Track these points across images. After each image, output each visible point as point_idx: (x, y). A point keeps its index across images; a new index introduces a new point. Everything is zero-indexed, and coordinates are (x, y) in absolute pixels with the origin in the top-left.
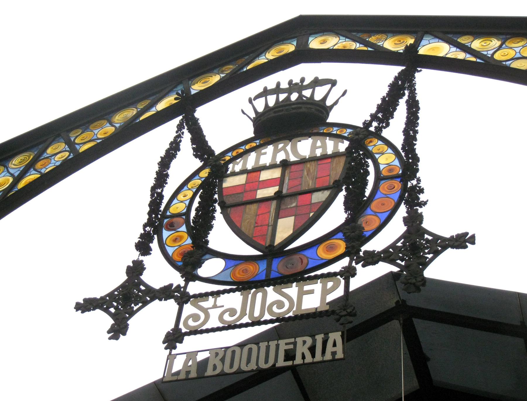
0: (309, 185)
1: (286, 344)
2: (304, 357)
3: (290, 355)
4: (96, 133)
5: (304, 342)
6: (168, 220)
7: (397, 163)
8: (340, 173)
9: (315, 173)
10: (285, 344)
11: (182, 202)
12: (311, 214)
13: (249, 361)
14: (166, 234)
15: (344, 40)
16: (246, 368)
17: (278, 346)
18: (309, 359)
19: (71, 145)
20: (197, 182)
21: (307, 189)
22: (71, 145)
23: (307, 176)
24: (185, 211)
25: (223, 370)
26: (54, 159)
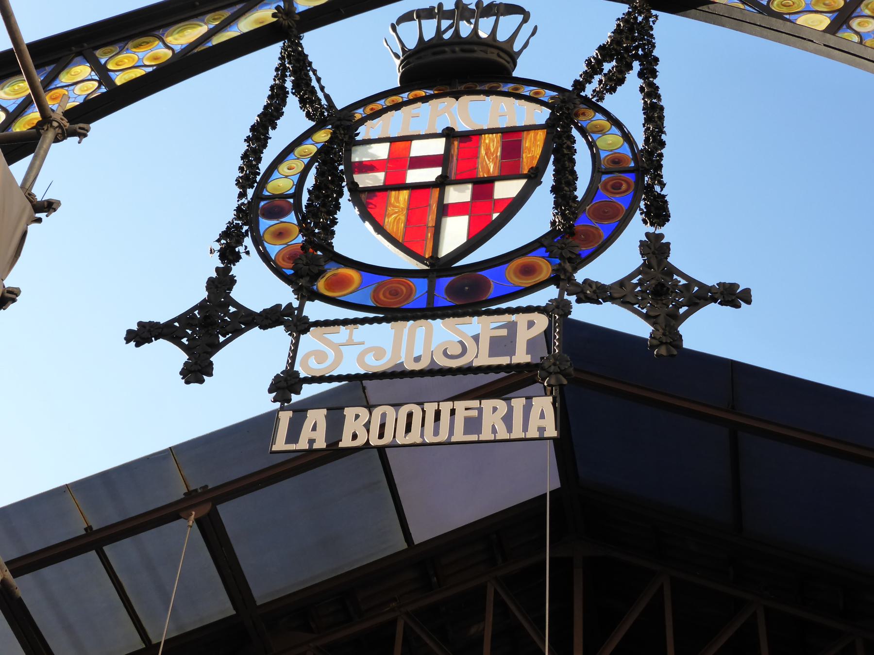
0: (489, 170)
2: (494, 431)
3: (473, 424)
6: (265, 202)
7: (627, 151)
8: (538, 157)
9: (499, 154)
11: (286, 177)
12: (495, 216)
13: (408, 429)
14: (265, 224)
17: (453, 412)
18: (503, 434)
19: (103, 74)
20: (310, 148)
21: (486, 176)
22: (103, 74)
23: (486, 157)
24: (292, 191)
26: (73, 90)
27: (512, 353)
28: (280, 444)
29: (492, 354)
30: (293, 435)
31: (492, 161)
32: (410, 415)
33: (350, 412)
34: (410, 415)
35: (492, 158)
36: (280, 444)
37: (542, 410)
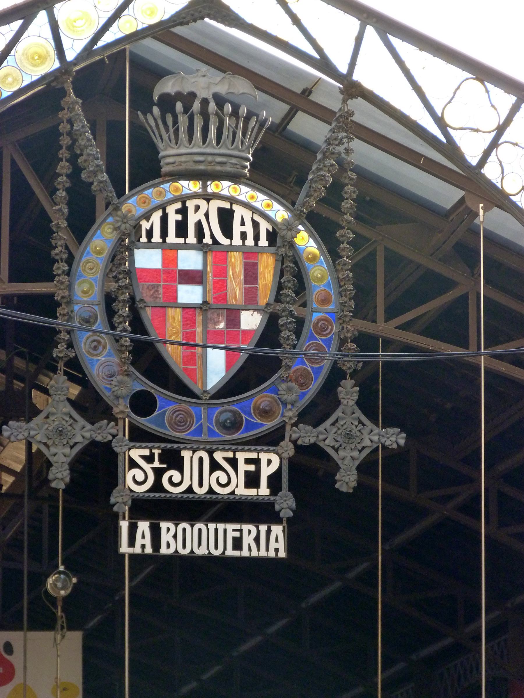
1: (234, 530)
2: (250, 549)
3: (238, 543)
5: (250, 532)
10: (231, 530)
13: (200, 544)
16: (199, 551)
17: (225, 530)
18: (254, 553)
25: (176, 551)
28: (124, 548)
30: (132, 543)
31: (238, 284)
32: (200, 530)
33: (164, 525)
34: (200, 530)
35: (237, 280)
37: (277, 534)
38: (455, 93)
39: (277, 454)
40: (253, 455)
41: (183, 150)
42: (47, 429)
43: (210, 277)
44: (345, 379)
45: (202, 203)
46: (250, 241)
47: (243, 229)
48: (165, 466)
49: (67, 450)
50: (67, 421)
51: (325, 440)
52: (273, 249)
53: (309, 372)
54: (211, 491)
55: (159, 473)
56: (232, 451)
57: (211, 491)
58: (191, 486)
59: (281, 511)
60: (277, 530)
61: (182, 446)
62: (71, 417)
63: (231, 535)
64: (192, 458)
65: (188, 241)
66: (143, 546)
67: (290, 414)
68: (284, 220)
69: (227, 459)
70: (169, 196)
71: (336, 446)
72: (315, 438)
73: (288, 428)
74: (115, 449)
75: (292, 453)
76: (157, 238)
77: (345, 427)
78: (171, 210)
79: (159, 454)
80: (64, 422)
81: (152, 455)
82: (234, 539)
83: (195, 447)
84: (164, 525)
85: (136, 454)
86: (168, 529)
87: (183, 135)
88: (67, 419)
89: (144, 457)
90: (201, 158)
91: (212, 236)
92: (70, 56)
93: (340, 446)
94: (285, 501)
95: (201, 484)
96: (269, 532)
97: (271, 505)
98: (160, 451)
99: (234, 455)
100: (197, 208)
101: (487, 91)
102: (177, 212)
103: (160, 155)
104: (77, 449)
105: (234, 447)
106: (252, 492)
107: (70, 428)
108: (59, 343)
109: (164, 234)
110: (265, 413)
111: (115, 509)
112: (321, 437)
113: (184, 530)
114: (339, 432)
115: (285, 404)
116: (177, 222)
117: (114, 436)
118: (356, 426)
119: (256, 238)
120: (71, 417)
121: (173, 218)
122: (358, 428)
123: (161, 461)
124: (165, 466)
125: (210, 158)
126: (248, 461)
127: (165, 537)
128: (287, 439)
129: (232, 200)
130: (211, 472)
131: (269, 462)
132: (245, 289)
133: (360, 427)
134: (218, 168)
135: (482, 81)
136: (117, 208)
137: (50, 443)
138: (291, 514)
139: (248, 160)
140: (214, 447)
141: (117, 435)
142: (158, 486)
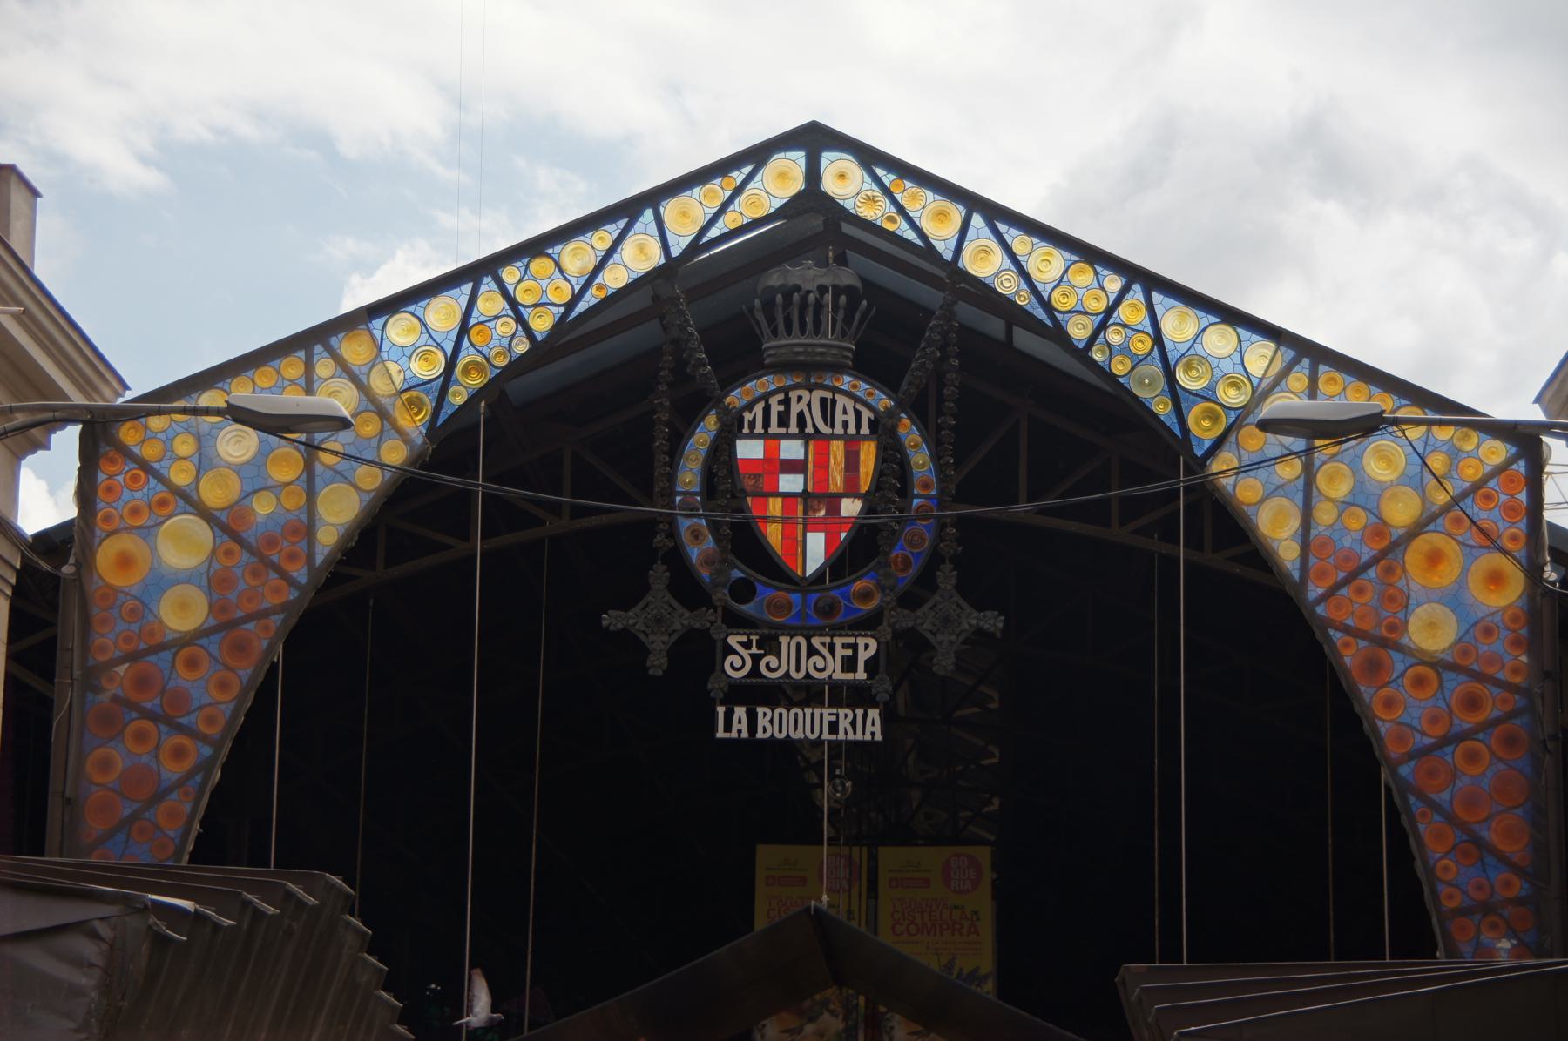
1: (830, 714)
2: (846, 733)
3: (834, 727)
4: (544, 289)
5: (846, 716)
12: (843, 535)
13: (796, 728)
15: (869, 187)
17: (821, 715)
18: (851, 737)
21: (835, 490)
27: (854, 669)
28: (720, 734)
29: (843, 671)
30: (728, 728)
32: (796, 714)
33: (760, 710)
34: (796, 714)
36: (720, 734)
38: (1062, 277)
39: (877, 640)
40: (851, 640)
41: (784, 342)
42: (646, 617)
43: (810, 466)
44: (944, 562)
45: (805, 394)
46: (852, 430)
47: (845, 418)
48: (762, 652)
49: (666, 638)
50: (666, 610)
51: (922, 624)
52: (875, 436)
53: (908, 558)
54: (808, 675)
55: (756, 659)
56: (829, 636)
57: (808, 675)
58: (788, 671)
59: (877, 694)
60: (874, 714)
61: (779, 632)
62: (671, 606)
63: (827, 719)
64: (789, 644)
65: (790, 432)
66: (739, 731)
67: (888, 599)
68: (886, 408)
69: (824, 644)
70: (773, 387)
71: (934, 631)
72: (913, 623)
73: (886, 612)
74: (713, 636)
75: (889, 637)
76: (759, 429)
77: (943, 610)
78: (774, 401)
79: (757, 640)
80: (663, 611)
81: (750, 641)
82: (831, 723)
83: (792, 633)
84: (760, 710)
85: (733, 641)
86: (765, 714)
87: (781, 327)
88: (666, 607)
89: (741, 644)
90: (801, 349)
91: (814, 426)
92: (675, 252)
93: (939, 629)
94: (881, 684)
95: (798, 669)
96: (865, 716)
97: (870, 687)
98: (758, 637)
99: (832, 640)
100: (800, 398)
101: (1096, 274)
102: (780, 402)
103: (764, 347)
104: (675, 637)
105: (831, 633)
106: (850, 676)
107: (668, 616)
108: (657, 533)
109: (766, 424)
110: (866, 596)
111: (712, 694)
112: (919, 621)
113: (781, 715)
114: (937, 616)
115: (882, 588)
116: (778, 412)
117: (712, 623)
118: (954, 611)
119: (858, 426)
120: (671, 606)
121: (776, 408)
122: (957, 612)
123: (759, 647)
124: (762, 652)
125: (810, 349)
126: (845, 646)
127: (762, 722)
128: (885, 623)
129: (835, 390)
130: (809, 656)
131: (867, 646)
132: (845, 475)
133: (958, 611)
134: (818, 358)
135: (1091, 264)
136: (720, 400)
137: (648, 631)
138: (888, 698)
139: (849, 350)
140: (811, 633)
141: (716, 622)
142: (755, 671)
